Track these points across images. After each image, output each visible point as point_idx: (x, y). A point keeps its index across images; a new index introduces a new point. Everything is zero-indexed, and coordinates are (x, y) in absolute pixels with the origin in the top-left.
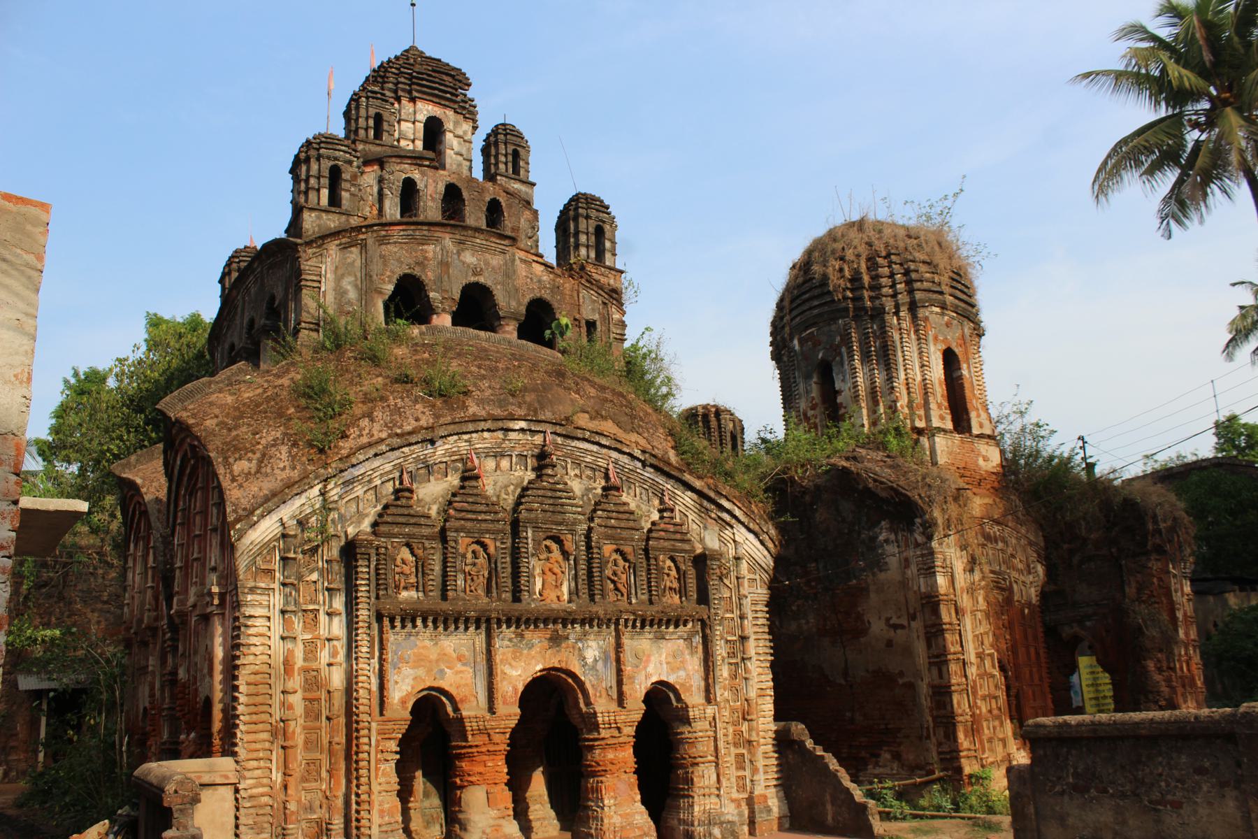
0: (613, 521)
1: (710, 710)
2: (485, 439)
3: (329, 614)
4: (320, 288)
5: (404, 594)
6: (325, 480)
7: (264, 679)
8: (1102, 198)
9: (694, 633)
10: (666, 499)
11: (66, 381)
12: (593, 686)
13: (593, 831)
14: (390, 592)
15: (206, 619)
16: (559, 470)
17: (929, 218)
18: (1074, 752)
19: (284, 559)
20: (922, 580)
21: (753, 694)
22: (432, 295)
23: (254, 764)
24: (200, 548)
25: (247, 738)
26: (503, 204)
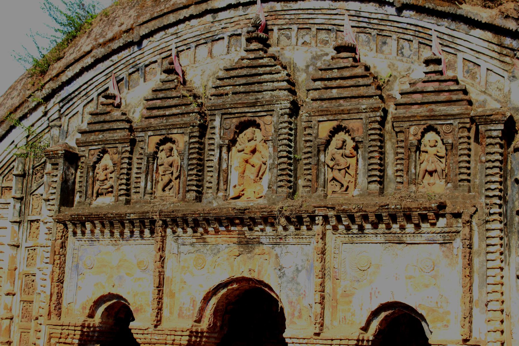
0: (334, 91)
2: (192, 27)
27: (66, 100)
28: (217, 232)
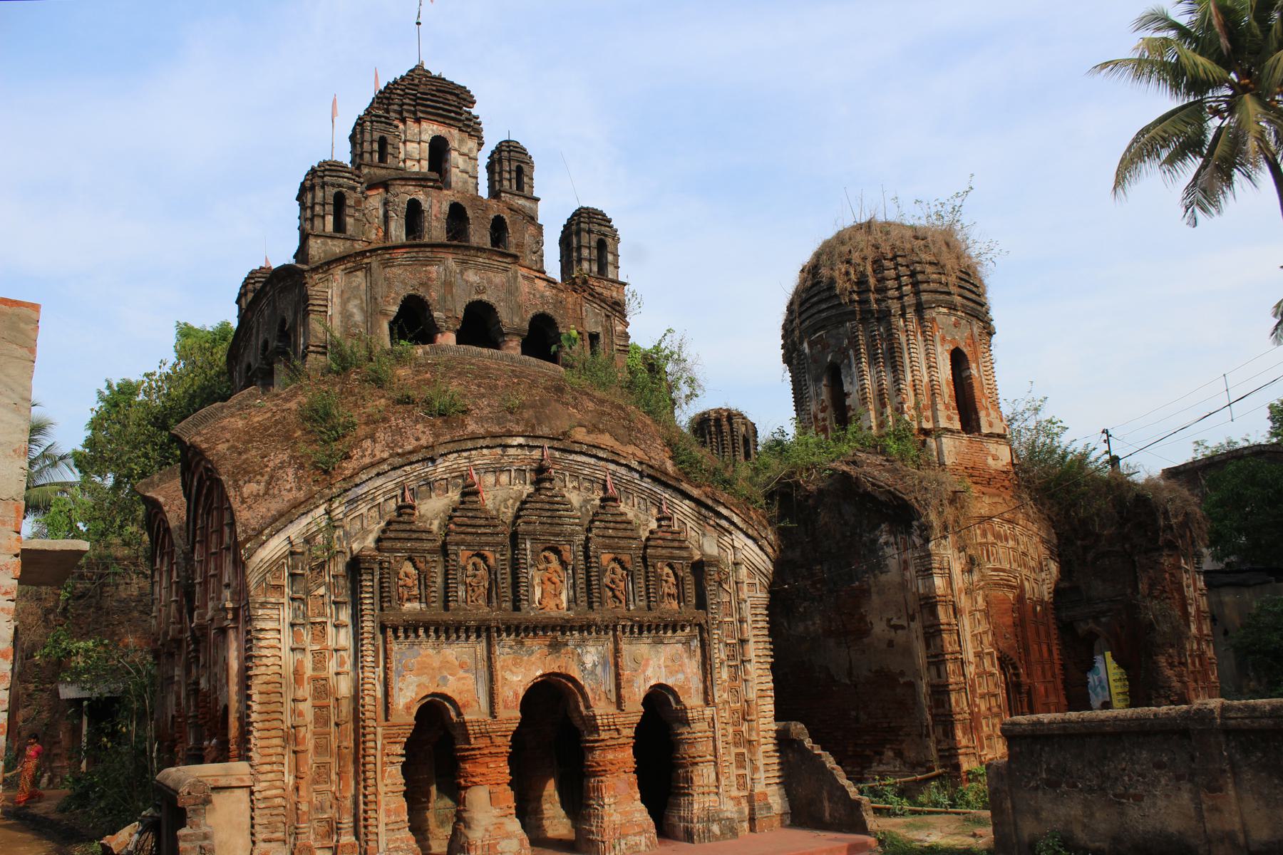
1: (708, 712)
3: (336, 626)
5: (408, 605)
6: (330, 500)
7: (275, 689)
8: (1119, 190)
9: (692, 637)
10: (664, 508)
11: (100, 392)
12: (592, 690)
13: (594, 829)
14: (394, 604)
15: (223, 631)
16: (558, 483)
17: (940, 217)
18: (1047, 749)
19: (292, 575)
20: (920, 581)
21: (752, 695)
22: (436, 314)
23: (267, 768)
24: (216, 565)
25: (260, 743)
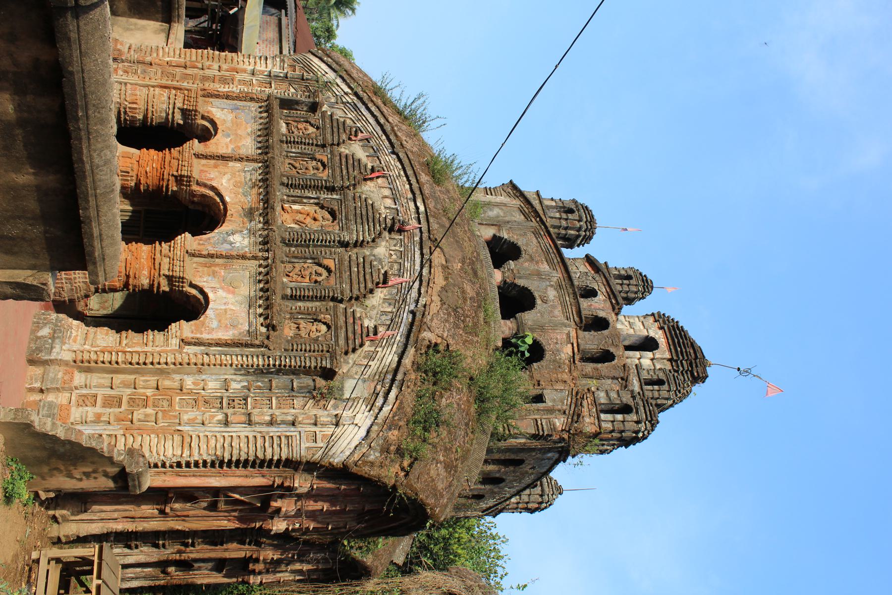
0: (356, 269)
1: (174, 342)
4: (487, 194)
5: (284, 125)
12: (209, 239)
23: (178, 52)
26: (613, 362)
27: (355, 107)
28: (260, 194)
